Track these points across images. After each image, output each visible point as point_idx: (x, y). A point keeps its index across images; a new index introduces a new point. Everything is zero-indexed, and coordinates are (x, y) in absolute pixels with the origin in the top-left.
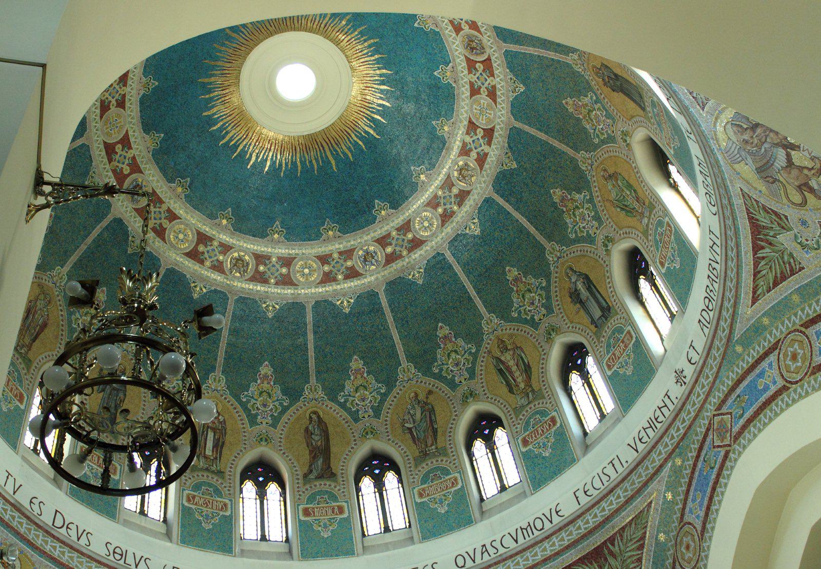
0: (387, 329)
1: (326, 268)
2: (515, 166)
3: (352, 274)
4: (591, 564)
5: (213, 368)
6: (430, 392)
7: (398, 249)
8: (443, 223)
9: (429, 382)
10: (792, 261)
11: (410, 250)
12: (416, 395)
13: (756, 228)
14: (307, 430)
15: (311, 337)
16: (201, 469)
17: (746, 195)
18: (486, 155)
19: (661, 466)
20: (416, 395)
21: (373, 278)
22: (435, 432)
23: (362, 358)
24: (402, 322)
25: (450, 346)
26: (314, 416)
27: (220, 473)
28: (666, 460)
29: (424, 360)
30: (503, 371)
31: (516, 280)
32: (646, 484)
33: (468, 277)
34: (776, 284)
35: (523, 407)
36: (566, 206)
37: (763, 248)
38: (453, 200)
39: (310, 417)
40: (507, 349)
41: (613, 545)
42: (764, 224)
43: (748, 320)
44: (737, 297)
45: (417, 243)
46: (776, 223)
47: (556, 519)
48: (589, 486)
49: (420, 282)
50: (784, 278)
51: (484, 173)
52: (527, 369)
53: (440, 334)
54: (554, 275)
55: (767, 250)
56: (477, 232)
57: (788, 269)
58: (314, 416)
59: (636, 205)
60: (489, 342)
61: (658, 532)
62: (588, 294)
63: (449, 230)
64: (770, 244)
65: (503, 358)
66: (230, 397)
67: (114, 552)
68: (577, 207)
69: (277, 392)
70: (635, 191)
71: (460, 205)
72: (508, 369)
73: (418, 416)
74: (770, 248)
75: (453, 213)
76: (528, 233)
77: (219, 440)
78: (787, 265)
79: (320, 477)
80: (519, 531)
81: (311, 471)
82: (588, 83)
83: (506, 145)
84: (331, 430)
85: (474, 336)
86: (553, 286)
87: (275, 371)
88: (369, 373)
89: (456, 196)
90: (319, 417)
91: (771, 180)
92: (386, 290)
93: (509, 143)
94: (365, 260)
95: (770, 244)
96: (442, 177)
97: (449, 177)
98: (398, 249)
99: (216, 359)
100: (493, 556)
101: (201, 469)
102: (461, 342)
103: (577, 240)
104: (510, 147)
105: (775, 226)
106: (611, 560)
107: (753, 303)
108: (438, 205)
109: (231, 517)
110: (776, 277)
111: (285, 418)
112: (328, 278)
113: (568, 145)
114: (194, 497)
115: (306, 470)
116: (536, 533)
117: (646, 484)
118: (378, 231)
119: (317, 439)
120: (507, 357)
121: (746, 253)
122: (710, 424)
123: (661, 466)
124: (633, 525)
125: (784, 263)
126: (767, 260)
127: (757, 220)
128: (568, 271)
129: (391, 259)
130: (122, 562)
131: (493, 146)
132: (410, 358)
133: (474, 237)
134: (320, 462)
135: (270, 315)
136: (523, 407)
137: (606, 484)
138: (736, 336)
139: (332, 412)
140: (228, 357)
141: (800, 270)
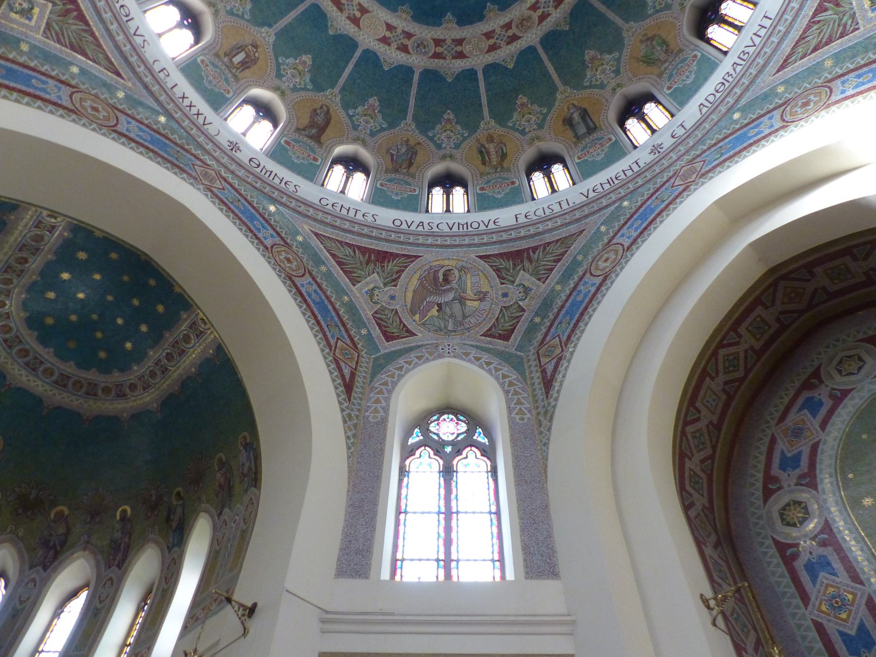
0: (408, 95)
1: (388, 34)
2: (567, 28)
3: (404, 49)
4: (508, 260)
5: (270, 26)
6: (419, 143)
7: (445, 52)
8: (488, 52)
9: (421, 138)
10: (849, 22)
11: (454, 58)
12: (408, 140)
14: (315, 110)
15: (351, 66)
16: (224, 63)
18: (549, 15)
19: (607, 206)
20: (408, 140)
21: (418, 62)
22: (410, 164)
23: (380, 101)
24: (421, 97)
25: (449, 126)
26: (325, 108)
27: (235, 76)
28: (614, 202)
29: (425, 124)
30: (483, 152)
31: (523, 105)
32: (586, 216)
33: (487, 92)
34: (815, 49)
35: (489, 173)
36: (592, 63)
37: (826, 10)
38: (505, 38)
39: (321, 107)
40: (493, 142)
41: (534, 252)
43: (762, 88)
44: (764, 66)
45: (461, 55)
47: (491, 226)
48: (532, 213)
49: (450, 80)
50: (830, 41)
51: (539, 27)
52: (504, 156)
53: (446, 116)
54: (554, 109)
55: (830, 12)
56: (511, 66)
58: (325, 108)
59: (663, 56)
60: (481, 134)
61: (579, 253)
62: (580, 120)
63: (490, 58)
65: (487, 146)
66: (272, 54)
67: (122, 6)
68: (602, 64)
69: (308, 78)
70: (667, 45)
71: (508, 43)
72: (488, 153)
73: (403, 150)
74: (832, 9)
75: (500, 47)
76: (550, 77)
77: (247, 63)
79: (310, 137)
80: (456, 225)
81: (304, 130)
83: (569, 11)
84: (332, 122)
85: (471, 126)
86: (550, 115)
87: (313, 65)
88: (379, 112)
89: (508, 37)
90: (328, 110)
92: (421, 73)
93: (572, 11)
94: (418, 46)
96: (507, 20)
97: (511, 22)
98: (445, 52)
99: (275, 23)
100: (426, 230)
101: (224, 63)
102: (459, 127)
103: (590, 87)
104: (571, 13)
106: (527, 264)
108: (493, 38)
109: (228, 99)
110: (821, 41)
111: (303, 93)
112: (384, 40)
113: (621, 17)
114: (207, 65)
115: (301, 127)
116: (470, 229)
117: (586, 216)
118: (437, 33)
119: (320, 120)
120: (491, 147)
121: (804, 17)
122: (675, 174)
123: (607, 206)
124: (559, 243)
125: (839, 25)
126: (821, 24)
128: (571, 106)
129: (436, 56)
130: (125, 19)
131: (558, 10)
132: (415, 118)
133: (506, 68)
134: (314, 131)
135: (331, 32)
136: (489, 173)
137: (547, 214)
138: (743, 102)
139: (339, 113)
140: (285, 31)
141: (852, 32)
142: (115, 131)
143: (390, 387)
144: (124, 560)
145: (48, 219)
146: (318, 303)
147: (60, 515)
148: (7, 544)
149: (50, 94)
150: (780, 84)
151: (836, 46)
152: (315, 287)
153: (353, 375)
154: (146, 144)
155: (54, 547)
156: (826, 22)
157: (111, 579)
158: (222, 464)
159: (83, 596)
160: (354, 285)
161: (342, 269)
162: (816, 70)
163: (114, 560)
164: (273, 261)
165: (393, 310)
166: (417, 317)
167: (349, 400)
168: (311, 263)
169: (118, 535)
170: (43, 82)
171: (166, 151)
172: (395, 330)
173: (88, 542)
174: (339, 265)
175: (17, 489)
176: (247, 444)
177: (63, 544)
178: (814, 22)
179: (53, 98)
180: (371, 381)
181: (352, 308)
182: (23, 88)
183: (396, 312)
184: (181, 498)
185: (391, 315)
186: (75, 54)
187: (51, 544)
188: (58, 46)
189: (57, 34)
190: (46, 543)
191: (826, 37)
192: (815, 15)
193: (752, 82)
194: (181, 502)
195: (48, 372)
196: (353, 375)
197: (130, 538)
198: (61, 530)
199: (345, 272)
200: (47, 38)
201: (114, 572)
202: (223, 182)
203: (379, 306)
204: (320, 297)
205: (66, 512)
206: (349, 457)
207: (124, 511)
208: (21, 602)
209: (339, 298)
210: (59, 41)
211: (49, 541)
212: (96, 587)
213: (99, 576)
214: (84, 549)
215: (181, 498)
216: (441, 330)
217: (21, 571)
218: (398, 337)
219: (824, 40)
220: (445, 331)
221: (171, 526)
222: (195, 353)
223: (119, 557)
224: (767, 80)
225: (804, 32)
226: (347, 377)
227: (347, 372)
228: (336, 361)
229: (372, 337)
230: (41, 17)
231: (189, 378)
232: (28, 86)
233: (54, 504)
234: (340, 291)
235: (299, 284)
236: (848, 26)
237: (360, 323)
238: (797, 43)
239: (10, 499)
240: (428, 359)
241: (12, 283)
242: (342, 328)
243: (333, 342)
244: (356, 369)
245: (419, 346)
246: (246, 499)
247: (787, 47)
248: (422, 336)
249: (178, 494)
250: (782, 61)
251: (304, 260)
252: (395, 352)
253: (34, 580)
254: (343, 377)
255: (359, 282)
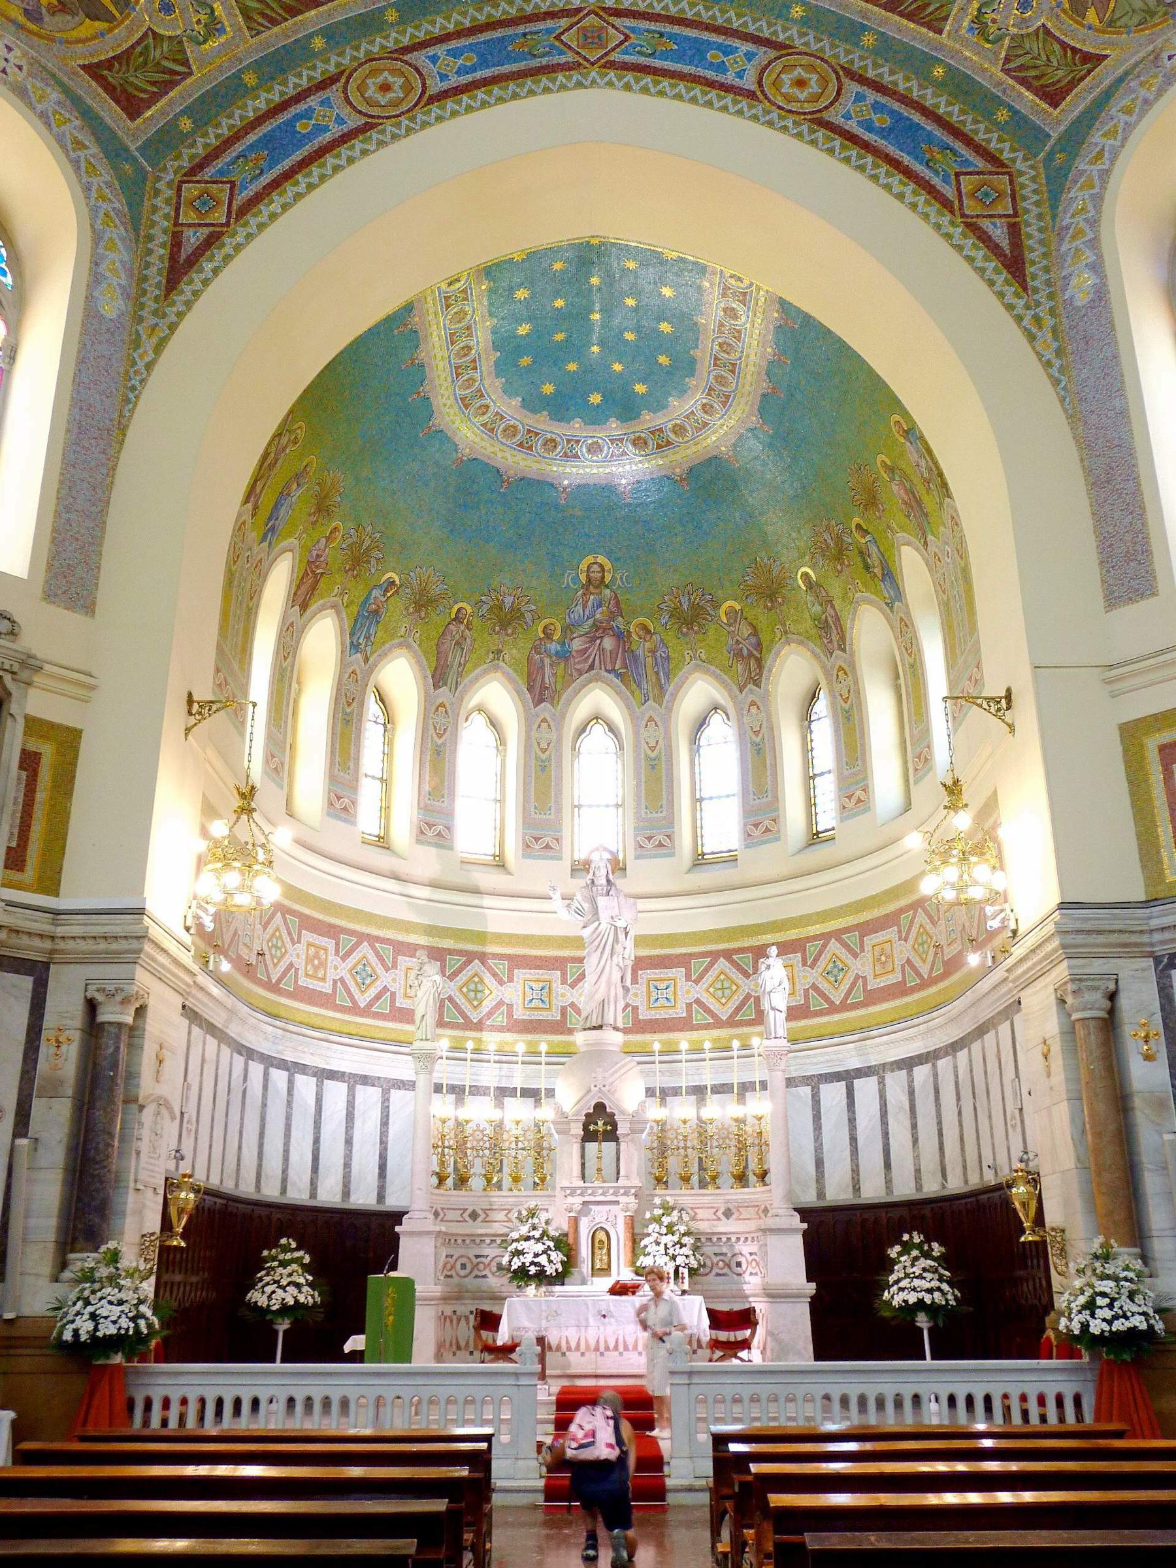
142: (432, 100)
143: (1092, 213)
144: (843, 639)
145: (452, 288)
146: (891, 129)
147: (731, 613)
148: (697, 674)
149: (326, 129)
152: (872, 96)
153: (1014, 230)
154: (478, 75)
155: (750, 655)
157: (841, 669)
158: (891, 470)
159: (822, 706)
160: (940, 32)
161: (901, 14)
163: (831, 642)
164: (774, 115)
165: (1037, 32)
166: (1092, 16)
167: (1025, 289)
168: (841, 48)
169: (817, 609)
170: (307, 114)
171: (510, 58)
172: (1061, 73)
173: (786, 632)
174: (892, 11)
175: (662, 606)
176: (905, 431)
177: (759, 646)
179: (335, 131)
180: (1054, 217)
181: (960, 85)
182: (298, 156)
183: (1047, 32)
184: (866, 532)
185: (1036, 46)
186: (300, 17)
187: (745, 652)
188: (276, 29)
189: (263, 14)
190: (738, 654)
194: (868, 538)
195: (594, 448)
196: (1014, 230)
197: (833, 606)
198: (746, 631)
199: (910, 17)
200: (258, 33)
201: (839, 658)
202: (617, 21)
203: (1007, 41)
204: (892, 112)
205: (738, 607)
206: (1062, 400)
207: (805, 575)
208: (757, 733)
209: (925, 78)
210: (274, 22)
211: (741, 650)
212: (830, 683)
213: (824, 668)
214: (788, 642)
215: (866, 532)
216: (1152, 14)
217: (733, 698)
218: (1072, 85)
220: (1162, 9)
221: (875, 575)
222: (756, 339)
223: (835, 638)
226: (1005, 244)
227: (999, 233)
228: (972, 228)
229: (1025, 118)
230: (230, 14)
231: (771, 363)
232: (300, 145)
233: (716, 605)
234: (918, 63)
235: (839, 120)
237: (983, 101)
239: (663, 622)
240: (1146, 101)
241: (475, 381)
242: (958, 146)
243: (949, 192)
244: (1016, 215)
245: (1121, 80)
246: (946, 517)
248: (1121, 53)
249: (858, 526)
251: (827, 55)
252: (1078, 121)
253: (753, 703)
254: (994, 248)
255: (946, 18)
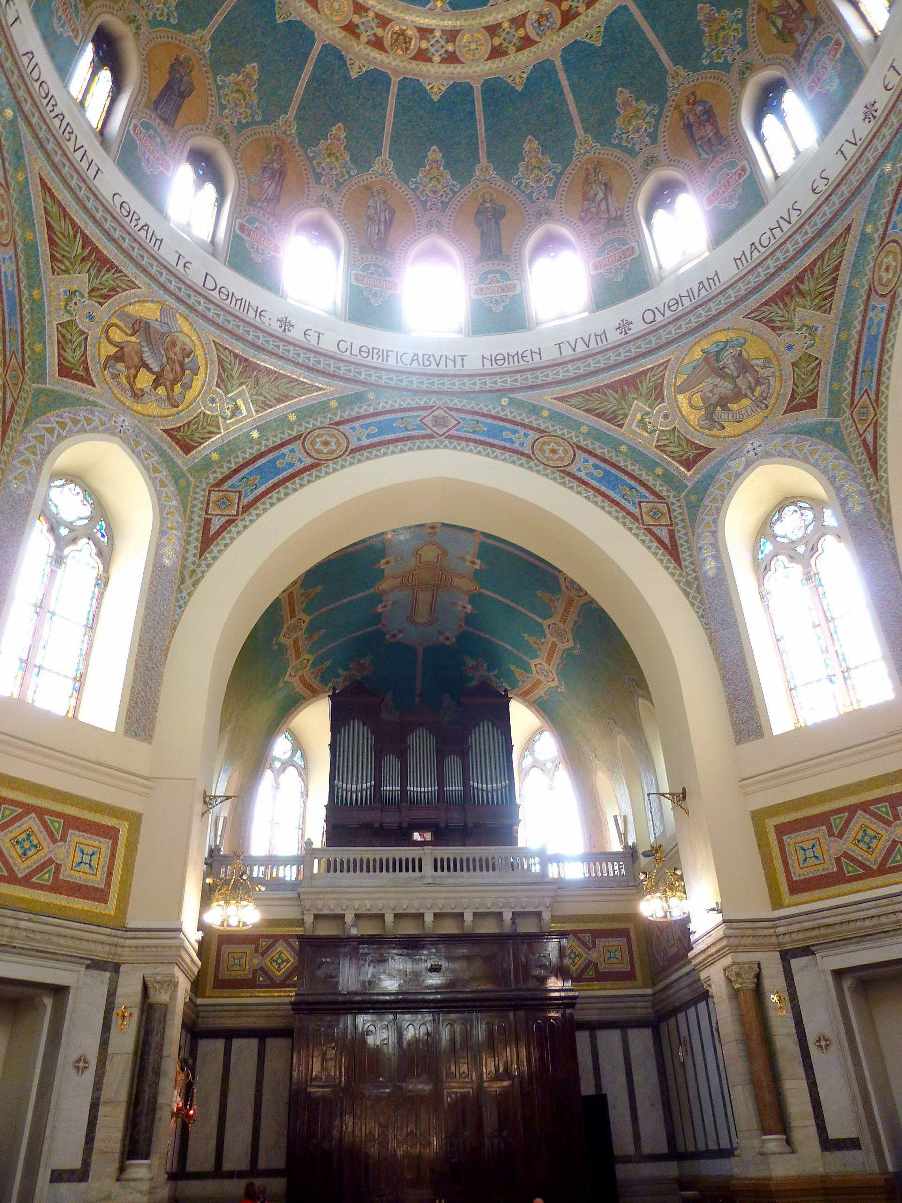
10: (63, 267)
13: (103, 263)
17: (133, 286)
37: (83, 247)
42: (102, 273)
43: (30, 155)
46: (99, 287)
50: (52, 242)
55: (80, 250)
57: (57, 255)
64: (83, 260)
78: (60, 257)
82: (184, 31)
91: (137, 327)
95: (83, 260)
105: (96, 284)
107: (41, 179)
121: (86, 223)
125: (63, 256)
127: (108, 270)
141: (52, 267)
150: (26, 178)
151: (44, 248)
156: (71, 243)
162: (28, 219)
178: (76, 232)
191: (58, 240)
192: (83, 234)
193: (42, 146)
219: (55, 238)
224: (37, 163)
225: (71, 220)
236: (59, 265)
238: (63, 208)
247: (63, 195)
250: (51, 187)
